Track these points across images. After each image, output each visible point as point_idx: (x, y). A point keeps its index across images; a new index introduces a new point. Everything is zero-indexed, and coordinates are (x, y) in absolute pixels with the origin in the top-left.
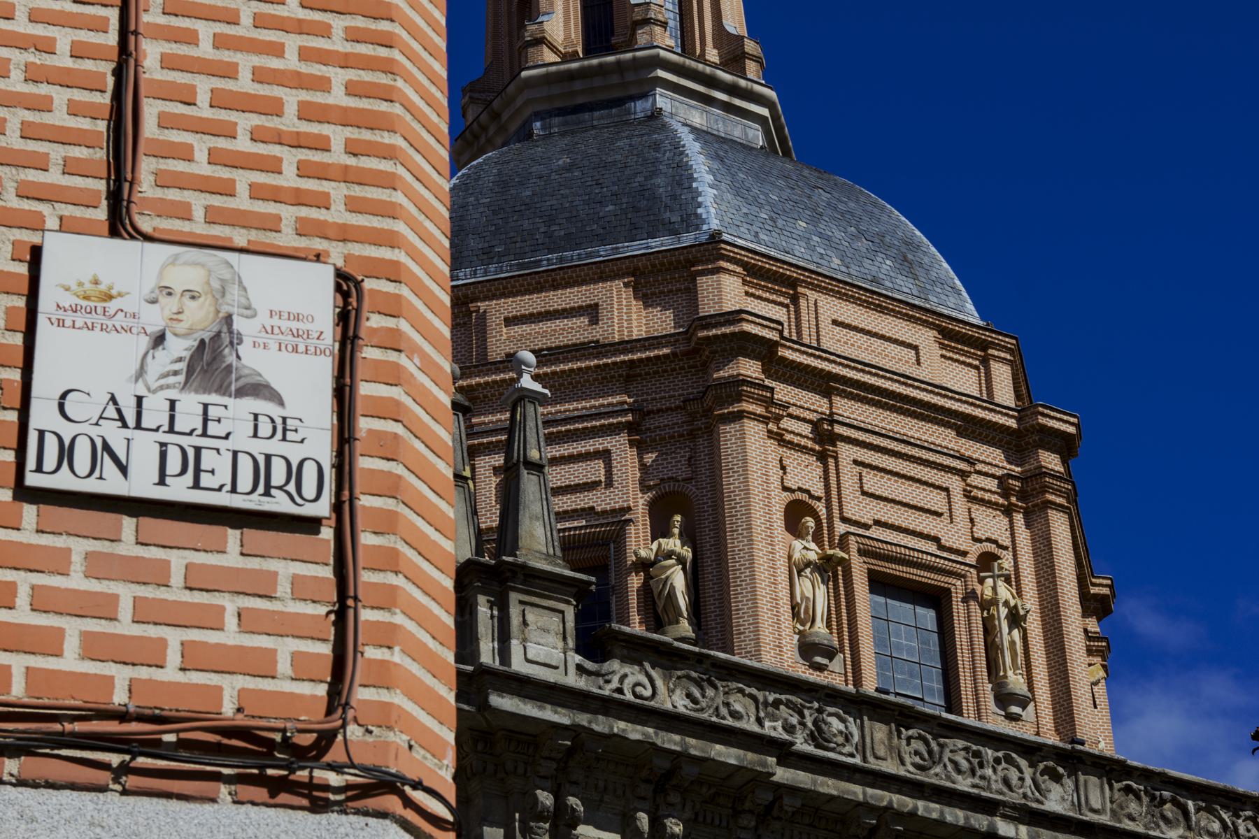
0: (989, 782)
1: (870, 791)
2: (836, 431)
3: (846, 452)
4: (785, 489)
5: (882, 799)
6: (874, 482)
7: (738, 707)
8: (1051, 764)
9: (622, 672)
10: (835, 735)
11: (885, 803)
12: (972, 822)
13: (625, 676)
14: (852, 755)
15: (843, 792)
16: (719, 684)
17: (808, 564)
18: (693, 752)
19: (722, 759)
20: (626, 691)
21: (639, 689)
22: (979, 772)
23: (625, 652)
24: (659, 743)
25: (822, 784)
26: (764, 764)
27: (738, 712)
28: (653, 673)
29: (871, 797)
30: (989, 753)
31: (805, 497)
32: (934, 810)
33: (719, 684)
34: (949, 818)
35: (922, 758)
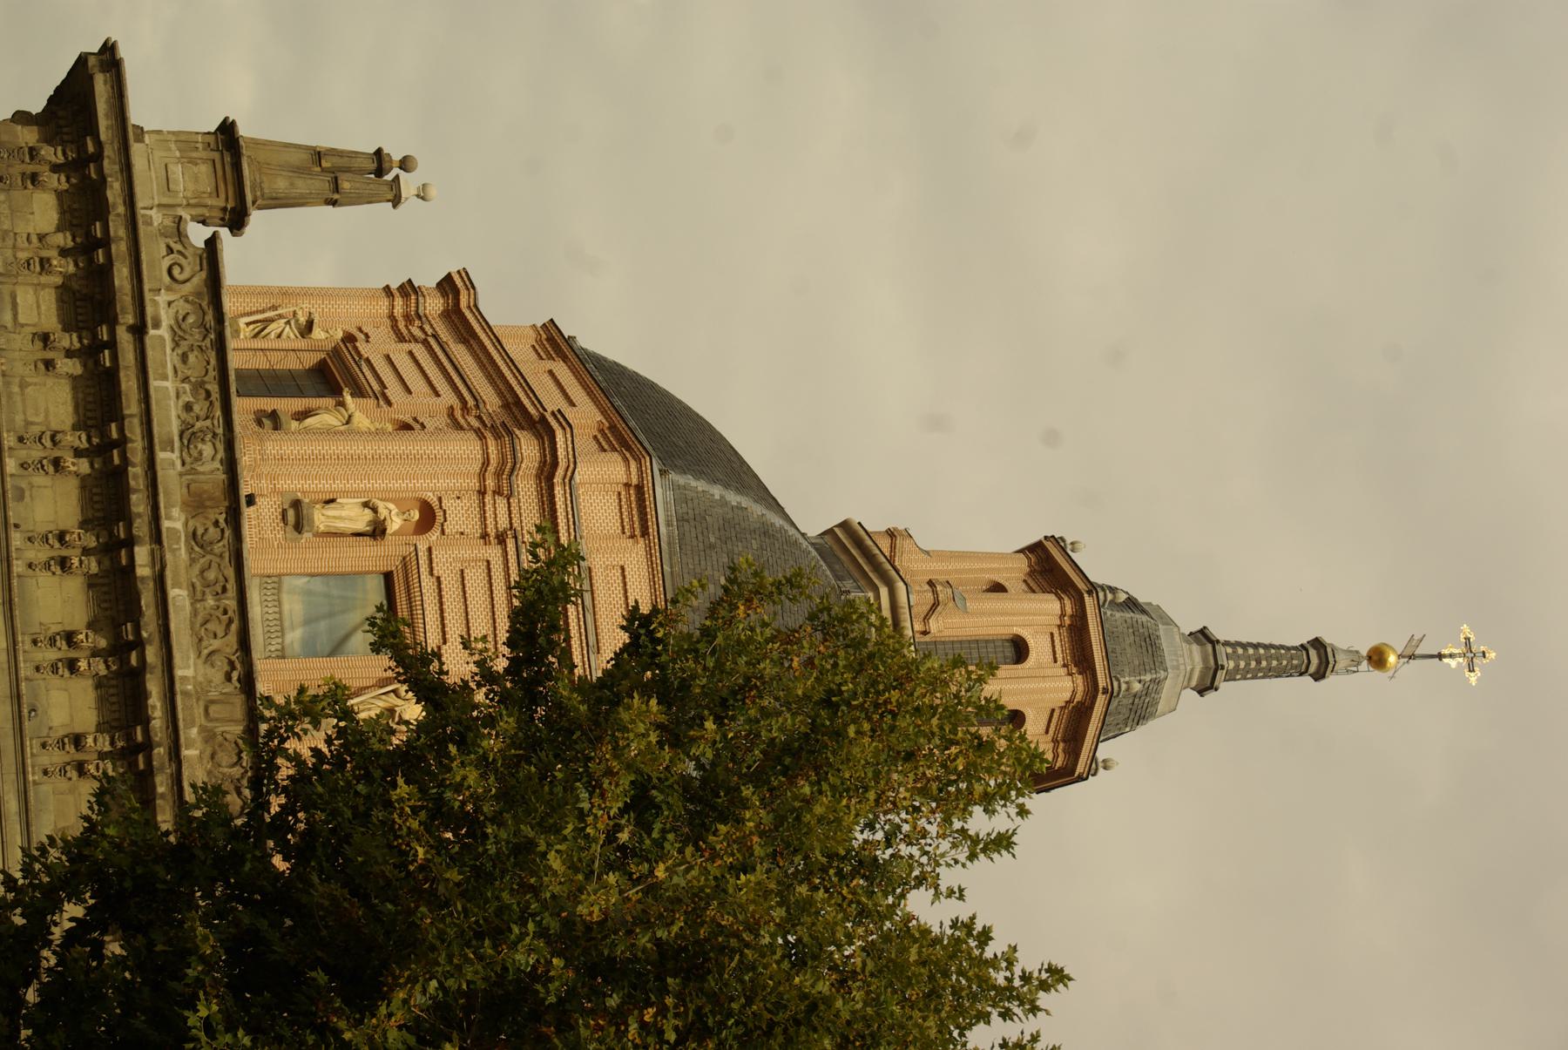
0: (202, 600)
1: (136, 421)
2: (508, 540)
3: (494, 553)
4: (440, 499)
5: (132, 432)
6: (475, 578)
7: (192, 358)
8: (238, 665)
9: (186, 254)
10: (196, 447)
11: (128, 435)
12: (138, 521)
13: (186, 258)
14: (183, 464)
15: (126, 395)
16: (208, 342)
17: (375, 510)
18: (113, 247)
19: (116, 273)
20: (172, 256)
21: (176, 271)
22: (207, 590)
23: (205, 255)
24: (111, 217)
25: (127, 376)
26: (124, 312)
27: (187, 357)
28: (196, 280)
29: (130, 422)
30: (231, 603)
31: (440, 518)
32: (137, 483)
33: (208, 342)
34: (134, 497)
35: (203, 535)
